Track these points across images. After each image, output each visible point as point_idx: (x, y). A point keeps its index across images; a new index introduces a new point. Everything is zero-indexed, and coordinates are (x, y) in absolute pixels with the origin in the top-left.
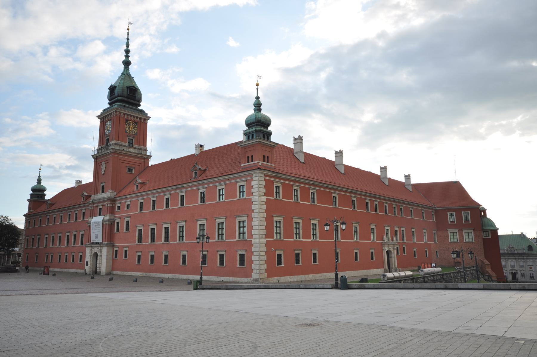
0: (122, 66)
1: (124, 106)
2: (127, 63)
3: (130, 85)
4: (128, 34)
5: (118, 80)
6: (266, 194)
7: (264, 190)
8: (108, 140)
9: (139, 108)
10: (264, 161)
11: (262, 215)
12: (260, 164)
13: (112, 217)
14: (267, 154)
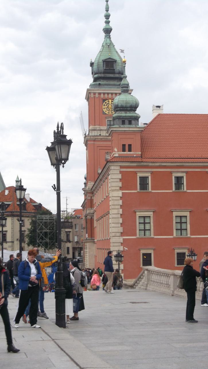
0: (103, 34)
1: (100, 84)
2: (108, 31)
6: (121, 188)
7: (120, 184)
10: (124, 150)
11: (115, 211)
12: (117, 155)
13: (92, 211)
14: (127, 144)
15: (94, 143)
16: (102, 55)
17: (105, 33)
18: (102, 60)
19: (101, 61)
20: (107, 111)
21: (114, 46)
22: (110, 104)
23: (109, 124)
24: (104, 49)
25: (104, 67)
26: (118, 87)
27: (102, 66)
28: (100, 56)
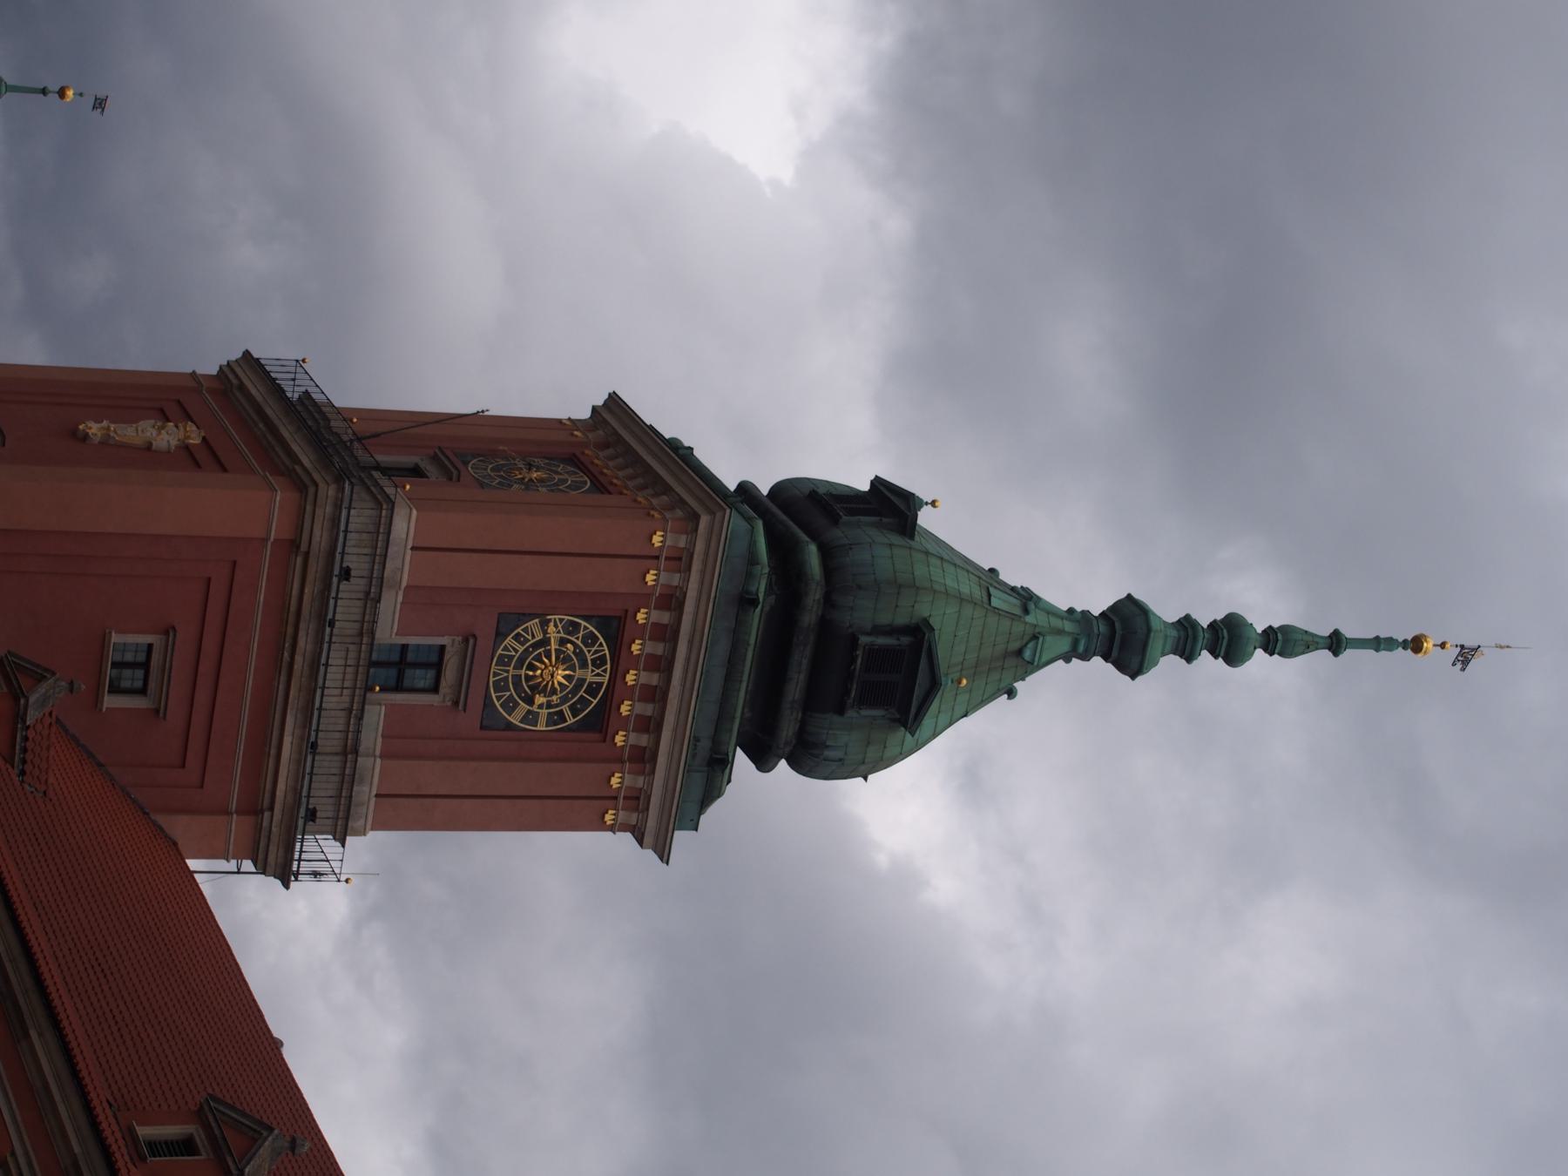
1: (746, 601)
3: (942, 652)
4: (1378, 644)
5: (966, 565)
8: (416, 472)
9: (742, 762)
15: (266, 540)
16: (968, 610)
17: (1103, 614)
18: (926, 621)
19: (926, 614)
20: (521, 649)
21: (1011, 693)
22: (579, 673)
23: (410, 657)
24: (1006, 623)
25: (877, 630)
26: (705, 744)
27: (884, 619)
28: (961, 600)
